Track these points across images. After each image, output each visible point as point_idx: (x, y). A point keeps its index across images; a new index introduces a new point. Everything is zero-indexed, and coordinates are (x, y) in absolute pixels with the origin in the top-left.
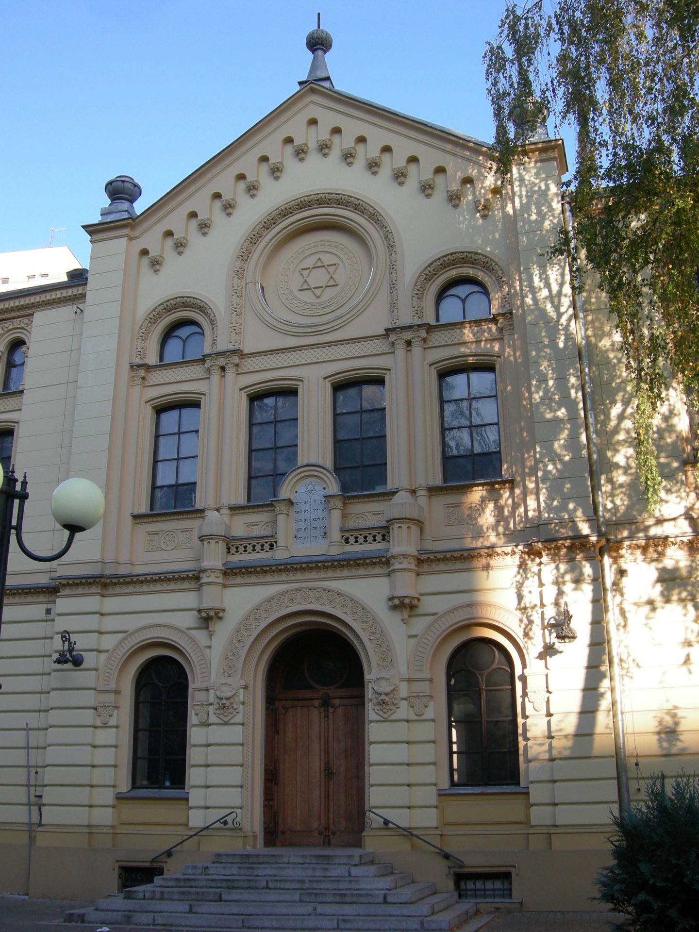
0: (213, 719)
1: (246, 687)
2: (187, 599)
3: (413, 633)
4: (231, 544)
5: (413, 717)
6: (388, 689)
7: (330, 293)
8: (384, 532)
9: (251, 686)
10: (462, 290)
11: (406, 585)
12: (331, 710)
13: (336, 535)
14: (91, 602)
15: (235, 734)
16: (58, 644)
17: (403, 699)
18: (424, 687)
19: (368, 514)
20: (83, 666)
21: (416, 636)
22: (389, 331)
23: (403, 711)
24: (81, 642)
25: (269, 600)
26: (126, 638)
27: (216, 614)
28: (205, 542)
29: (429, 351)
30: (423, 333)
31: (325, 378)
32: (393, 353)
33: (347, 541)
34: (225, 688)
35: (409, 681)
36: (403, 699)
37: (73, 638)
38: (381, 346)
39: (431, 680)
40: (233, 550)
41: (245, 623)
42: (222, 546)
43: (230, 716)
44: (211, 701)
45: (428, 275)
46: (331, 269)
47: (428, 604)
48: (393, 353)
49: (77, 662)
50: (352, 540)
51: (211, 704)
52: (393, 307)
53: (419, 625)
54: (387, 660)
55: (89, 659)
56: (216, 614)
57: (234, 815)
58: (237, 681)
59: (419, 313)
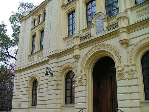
1: (85, 75)
3: (128, 51)
4: (82, 39)
9: (87, 75)
11: (124, 36)
13: (105, 29)
14: (55, 60)
16: (45, 70)
17: (126, 72)
18: (132, 68)
19: (113, 21)
20: (53, 75)
23: (127, 76)
24: (53, 70)
25: (90, 50)
26: (61, 67)
27: (78, 57)
33: (108, 30)
34: (80, 76)
35: (128, 66)
36: (126, 72)
39: (135, 65)
41: (85, 58)
42: (79, 40)
47: (132, 42)
49: (52, 74)
50: (110, 29)
54: (120, 61)
55: (55, 74)
56: (78, 57)
57: (82, 111)
58: (83, 73)
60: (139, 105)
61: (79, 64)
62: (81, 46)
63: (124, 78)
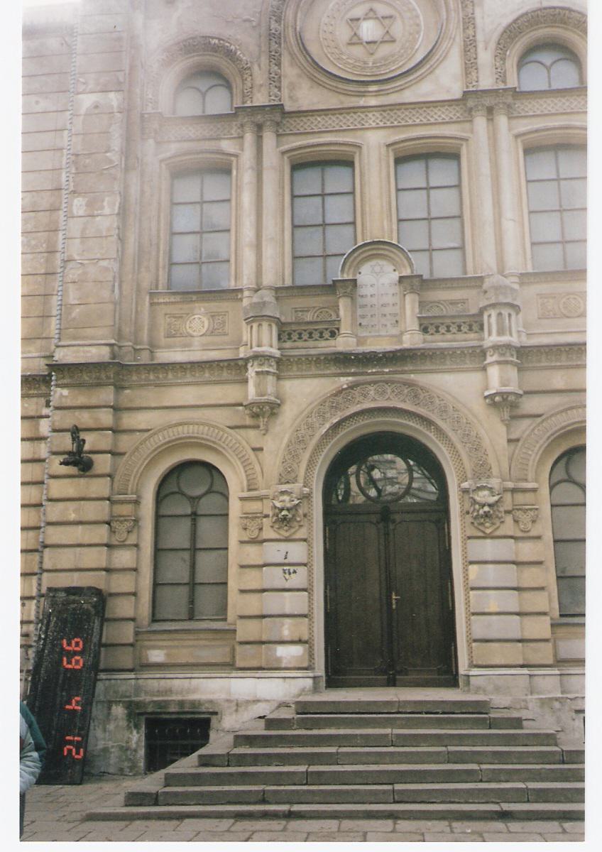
0: (268, 533)
2: (230, 393)
3: (513, 436)
5: (519, 534)
6: (492, 500)
7: (384, 50)
8: (476, 323)
10: (547, 57)
12: (391, 527)
13: (411, 323)
15: (297, 552)
21: (518, 440)
22: (466, 94)
23: (508, 527)
28: (255, 326)
29: (514, 122)
30: (510, 100)
31: (388, 146)
32: (471, 121)
34: (286, 498)
35: (514, 491)
37: (82, 435)
38: (454, 113)
40: (285, 337)
43: (293, 530)
44: (266, 512)
45: (511, 32)
46: (387, 22)
48: (471, 121)
51: (267, 516)
52: (470, 65)
53: (523, 427)
55: (103, 463)
59: (502, 77)
60: (547, 633)
61: (276, 441)
62: (283, 366)
63: (498, 533)
